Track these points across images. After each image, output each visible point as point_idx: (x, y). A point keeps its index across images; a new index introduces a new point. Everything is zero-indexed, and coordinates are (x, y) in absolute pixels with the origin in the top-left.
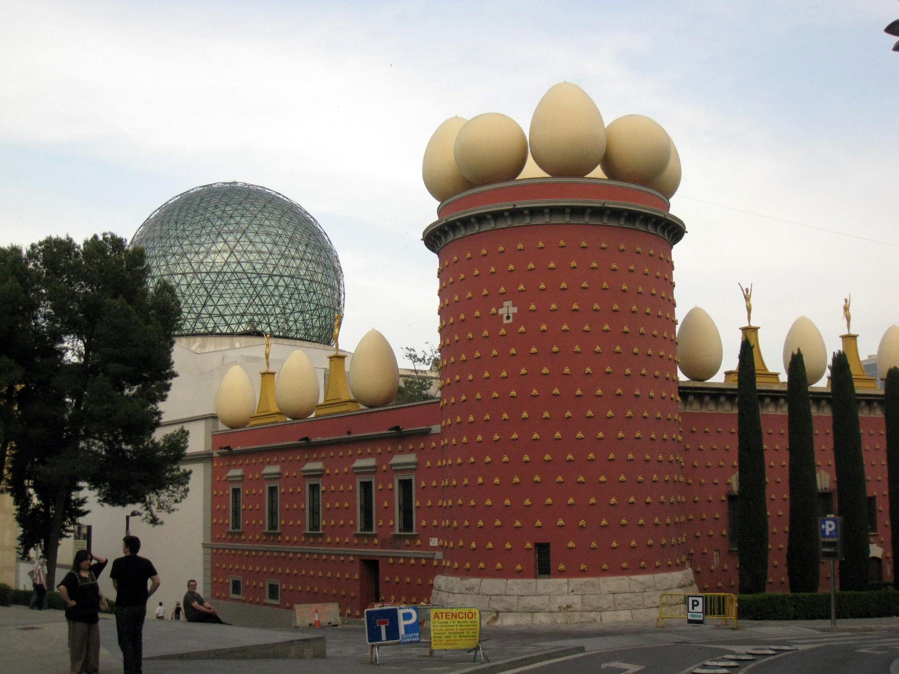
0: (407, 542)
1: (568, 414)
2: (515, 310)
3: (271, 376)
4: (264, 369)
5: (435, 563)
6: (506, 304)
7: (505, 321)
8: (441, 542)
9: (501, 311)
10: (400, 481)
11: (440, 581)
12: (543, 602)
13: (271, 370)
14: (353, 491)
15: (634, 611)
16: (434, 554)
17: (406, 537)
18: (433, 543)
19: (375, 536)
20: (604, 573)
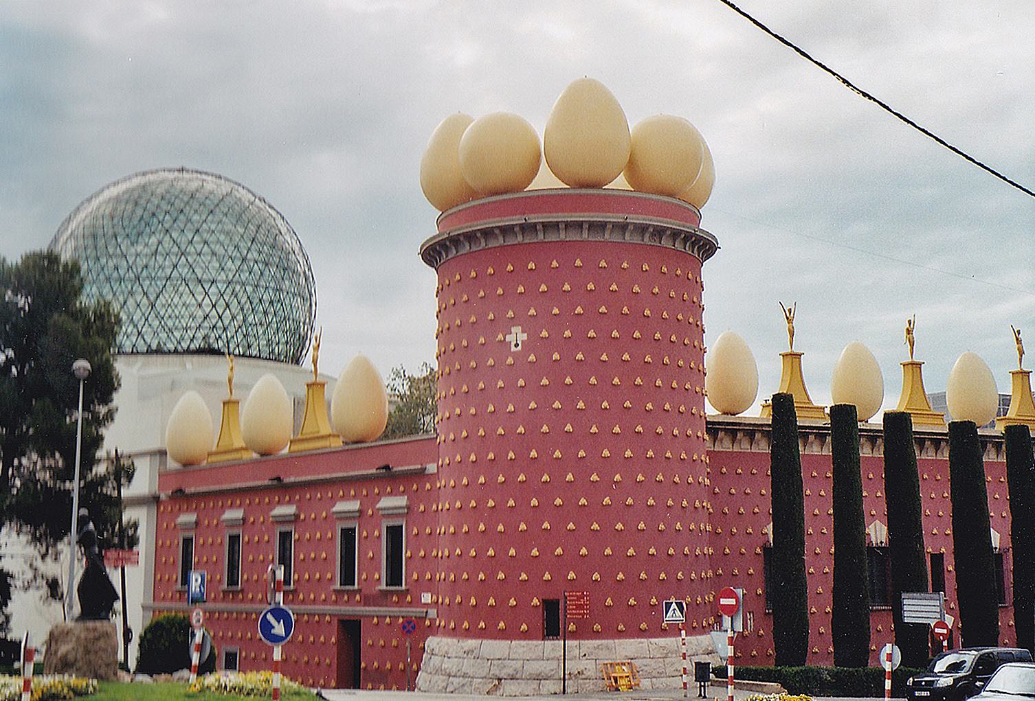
1: (582, 453)
2: (524, 337)
3: (236, 405)
4: (227, 398)
5: (428, 623)
6: (514, 330)
7: (513, 349)
8: (435, 597)
9: (508, 338)
11: (432, 642)
12: (552, 668)
13: (234, 398)
15: (654, 680)
16: (427, 612)
17: (392, 593)
19: (355, 592)
20: (620, 635)
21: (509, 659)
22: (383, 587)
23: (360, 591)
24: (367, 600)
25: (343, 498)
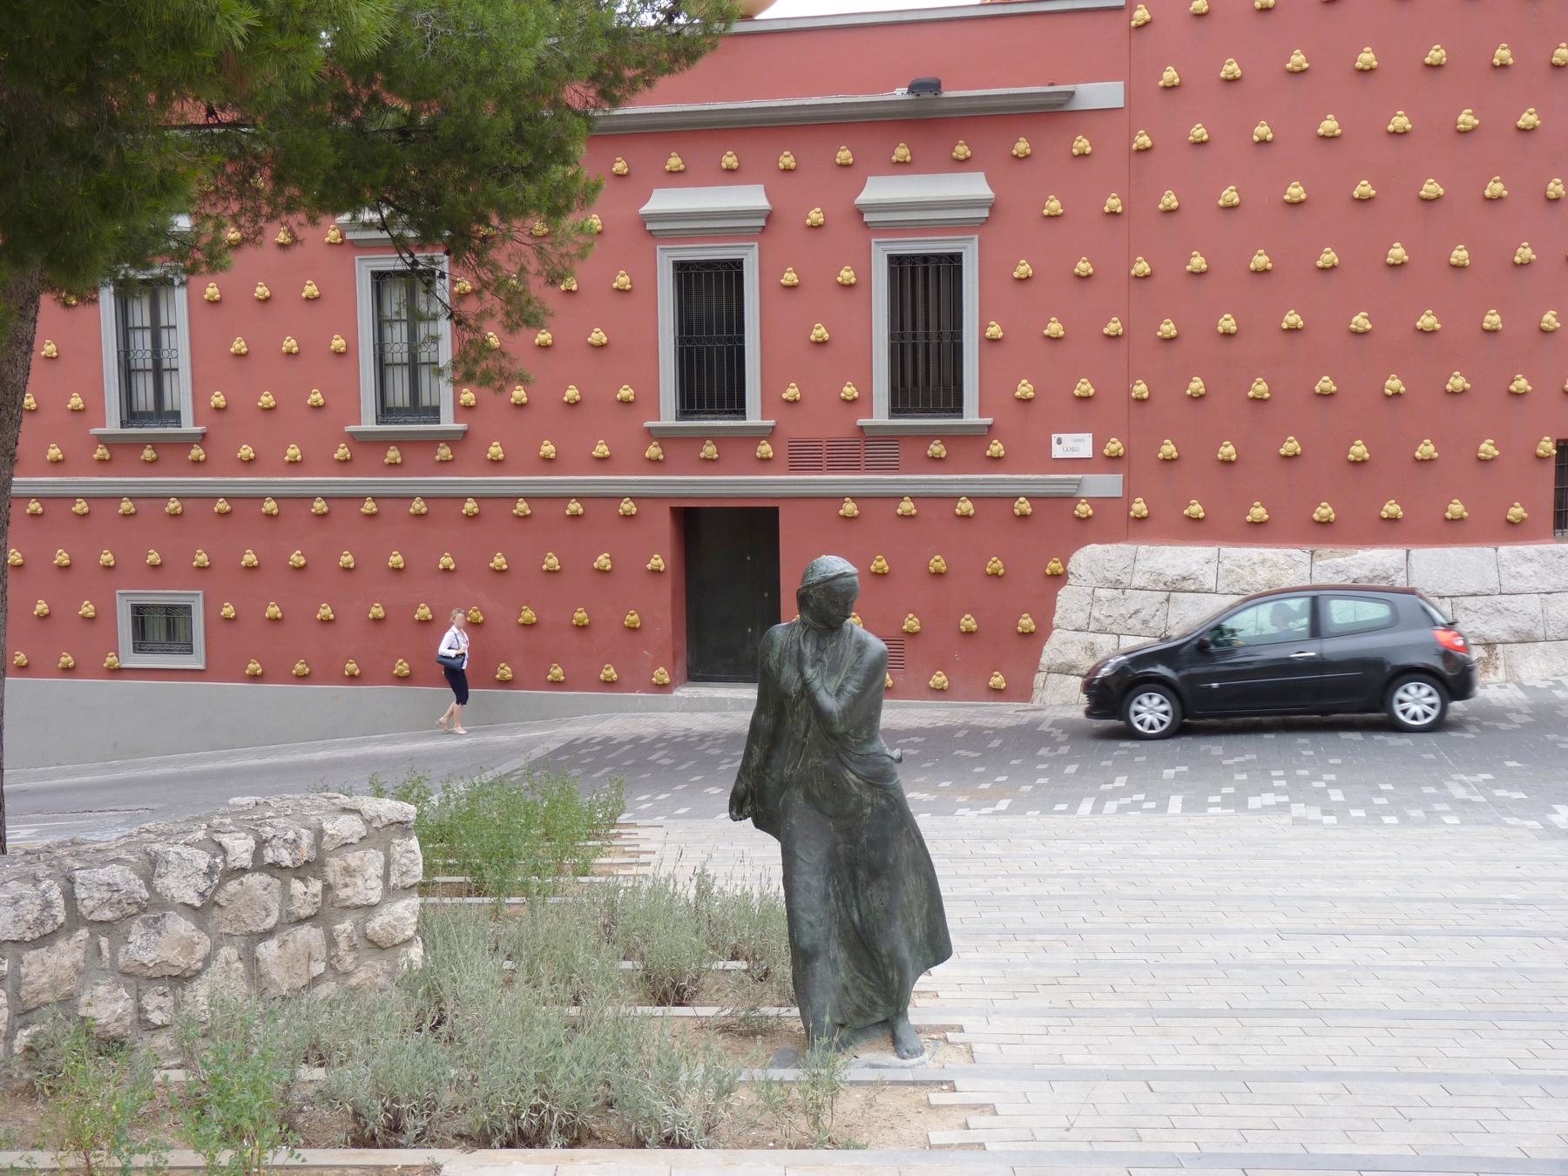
0: (937, 448)
10: (896, 262)
11: (1090, 559)
14: (638, 295)
16: (1079, 483)
17: (927, 436)
18: (1072, 450)
19: (756, 435)
21: (1501, 594)
22: (880, 415)
23: (769, 434)
24: (802, 456)
25: (676, 178)
